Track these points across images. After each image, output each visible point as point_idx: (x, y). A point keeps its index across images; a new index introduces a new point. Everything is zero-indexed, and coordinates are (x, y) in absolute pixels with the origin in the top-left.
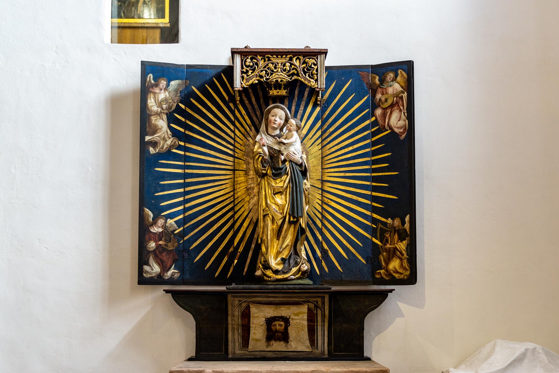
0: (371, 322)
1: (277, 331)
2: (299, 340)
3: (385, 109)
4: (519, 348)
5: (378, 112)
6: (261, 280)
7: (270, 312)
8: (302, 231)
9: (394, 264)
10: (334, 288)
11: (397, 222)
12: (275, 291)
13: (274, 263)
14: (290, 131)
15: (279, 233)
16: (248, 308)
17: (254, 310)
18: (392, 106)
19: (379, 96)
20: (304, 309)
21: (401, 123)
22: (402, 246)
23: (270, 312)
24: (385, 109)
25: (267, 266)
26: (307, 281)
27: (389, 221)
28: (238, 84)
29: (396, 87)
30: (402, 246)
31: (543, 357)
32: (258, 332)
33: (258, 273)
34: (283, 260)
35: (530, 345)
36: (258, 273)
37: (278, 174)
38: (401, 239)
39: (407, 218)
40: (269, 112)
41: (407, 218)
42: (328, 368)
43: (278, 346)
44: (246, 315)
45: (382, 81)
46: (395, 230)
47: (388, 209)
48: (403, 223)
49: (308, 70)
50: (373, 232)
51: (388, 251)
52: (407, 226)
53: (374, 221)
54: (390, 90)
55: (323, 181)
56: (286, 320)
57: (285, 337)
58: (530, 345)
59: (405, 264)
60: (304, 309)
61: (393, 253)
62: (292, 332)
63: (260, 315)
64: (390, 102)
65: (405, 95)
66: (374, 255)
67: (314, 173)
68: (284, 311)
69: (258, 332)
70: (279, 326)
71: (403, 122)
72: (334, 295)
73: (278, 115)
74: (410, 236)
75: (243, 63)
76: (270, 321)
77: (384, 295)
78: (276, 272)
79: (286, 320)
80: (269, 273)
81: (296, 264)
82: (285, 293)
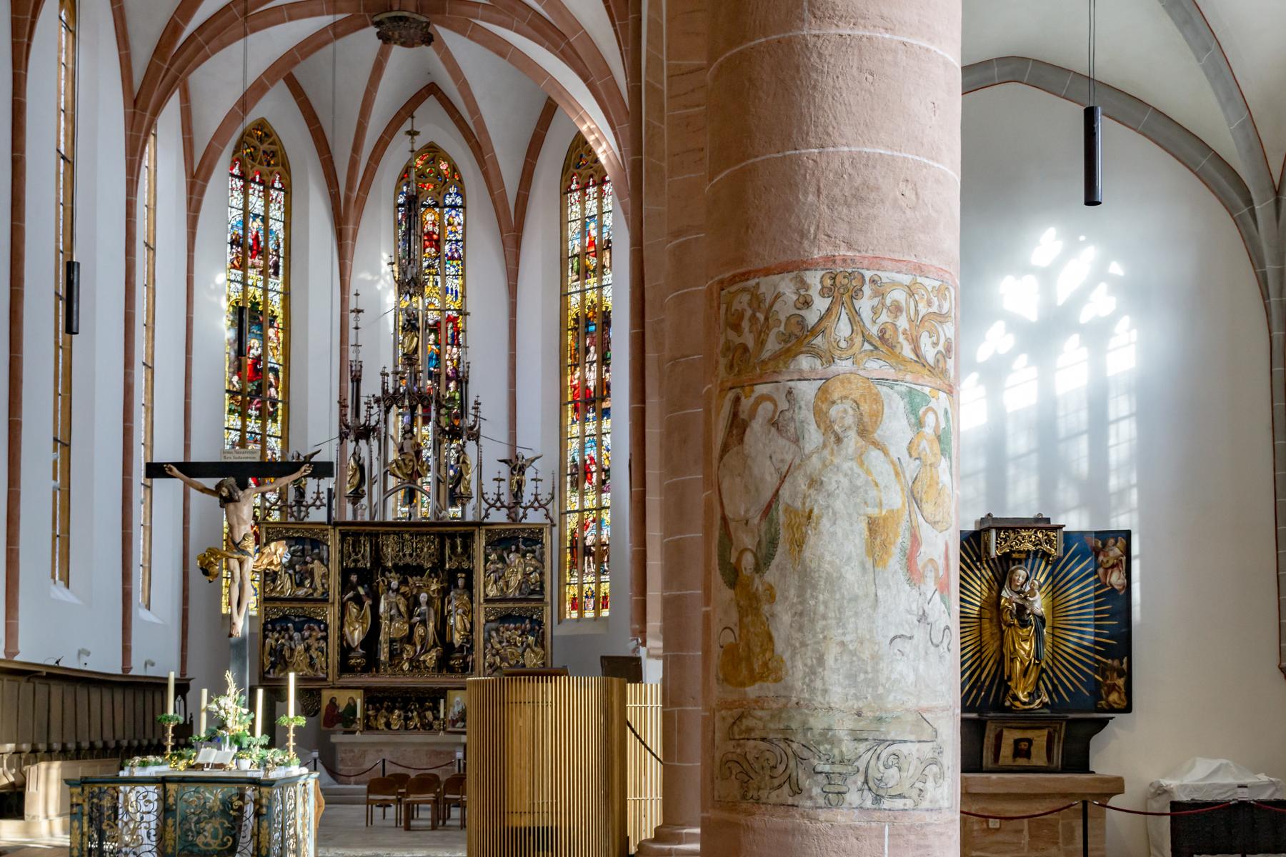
0: (1095, 742)
1: (1021, 750)
2: (1038, 758)
3: (1106, 569)
4: (1216, 763)
5: (1101, 571)
6: (1009, 709)
7: (1018, 734)
8: (1043, 670)
9: (1114, 697)
10: (1071, 716)
11: (1116, 663)
12: (1026, 718)
13: (1021, 696)
14: (1032, 589)
15: (1025, 673)
16: (1001, 732)
17: (1006, 733)
18: (1113, 566)
19: (1101, 558)
20: (1045, 732)
21: (1120, 581)
22: (1121, 682)
23: (1018, 734)
24: (1106, 569)
25: (1016, 698)
26: (1046, 711)
27: (1109, 661)
28: (994, 553)
29: (1116, 551)
30: (1121, 682)
31: (1234, 769)
32: (1007, 750)
33: (1007, 704)
34: (1030, 694)
35: (1224, 761)
36: (1007, 704)
37: (1024, 624)
38: (1120, 676)
39: (1125, 660)
40: (1013, 572)
41: (1125, 660)
42: (984, 805)
43: (1022, 762)
44: (999, 738)
45: (1104, 545)
46: (1113, 669)
47: (1108, 652)
48: (1122, 664)
49: (1049, 542)
50: (1096, 670)
51: (1109, 686)
52: (1125, 666)
53: (1097, 661)
54: (1111, 554)
55: (1054, 628)
56: (1030, 741)
57: (1027, 754)
58: (1224, 761)
59: (1123, 697)
60: (1045, 732)
61: (1113, 688)
62: (1033, 750)
63: (1009, 737)
64: (1111, 563)
65: (1124, 558)
66: (1097, 691)
67: (1049, 623)
68: (1029, 734)
69: (1007, 750)
70: (1024, 745)
71: (1123, 581)
72: (1070, 722)
73: (1021, 574)
74: (1128, 675)
75: (998, 535)
76: (1017, 742)
77: (1104, 722)
78: (1024, 703)
79: (1030, 741)
80: (1017, 703)
81: (1039, 697)
82: (1029, 720)
